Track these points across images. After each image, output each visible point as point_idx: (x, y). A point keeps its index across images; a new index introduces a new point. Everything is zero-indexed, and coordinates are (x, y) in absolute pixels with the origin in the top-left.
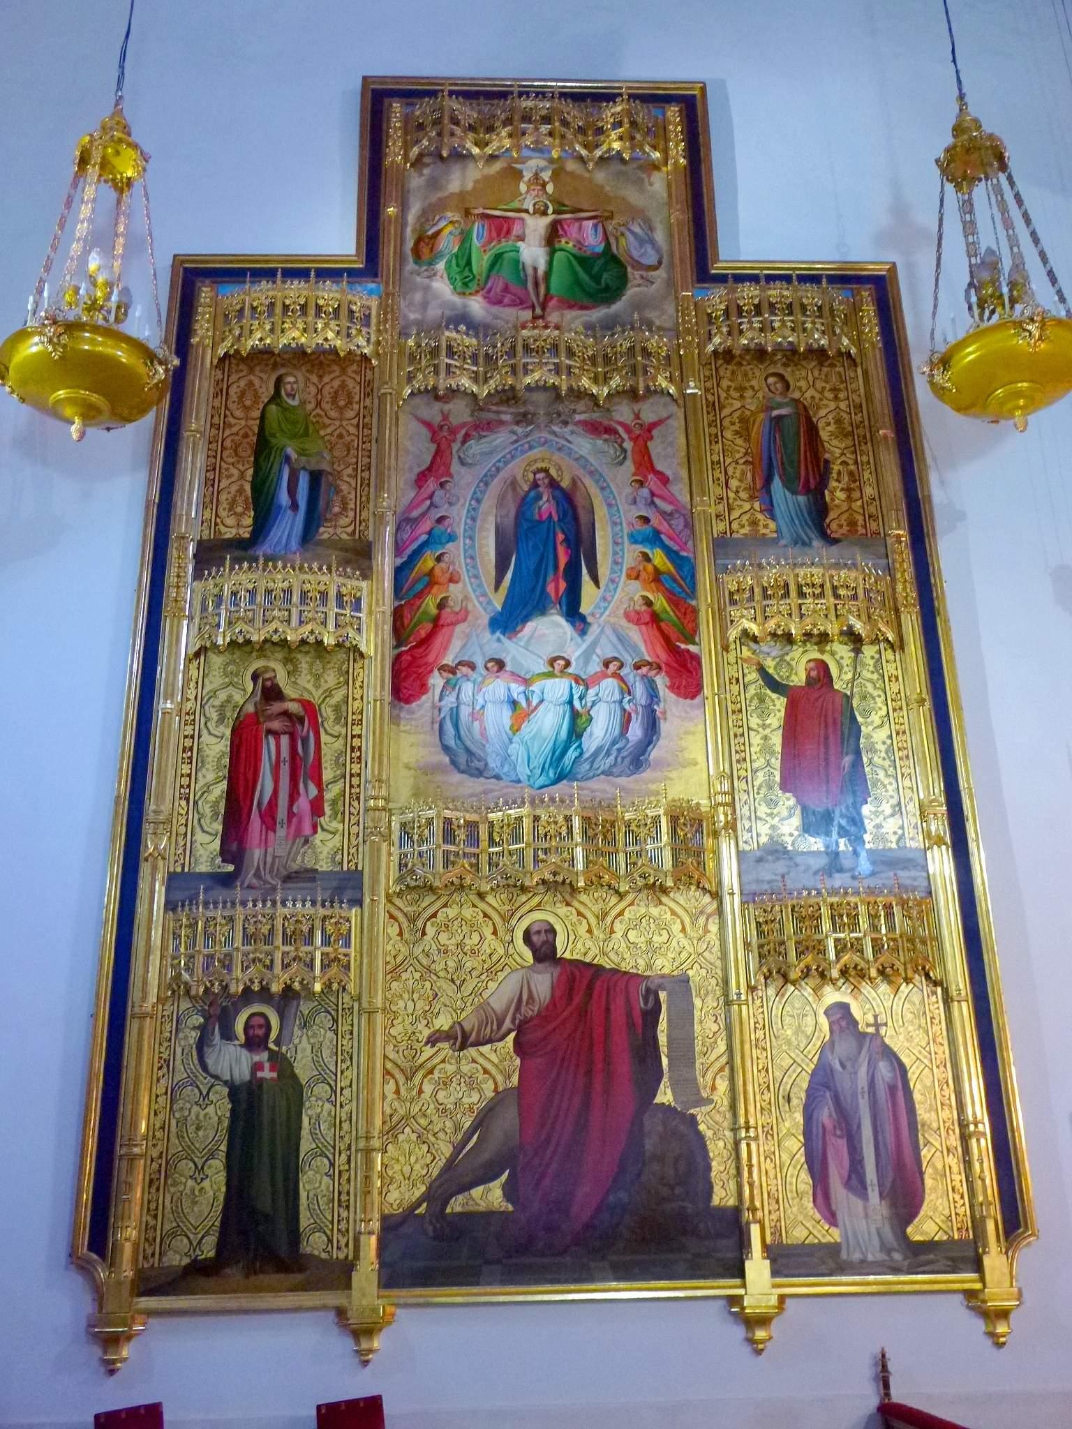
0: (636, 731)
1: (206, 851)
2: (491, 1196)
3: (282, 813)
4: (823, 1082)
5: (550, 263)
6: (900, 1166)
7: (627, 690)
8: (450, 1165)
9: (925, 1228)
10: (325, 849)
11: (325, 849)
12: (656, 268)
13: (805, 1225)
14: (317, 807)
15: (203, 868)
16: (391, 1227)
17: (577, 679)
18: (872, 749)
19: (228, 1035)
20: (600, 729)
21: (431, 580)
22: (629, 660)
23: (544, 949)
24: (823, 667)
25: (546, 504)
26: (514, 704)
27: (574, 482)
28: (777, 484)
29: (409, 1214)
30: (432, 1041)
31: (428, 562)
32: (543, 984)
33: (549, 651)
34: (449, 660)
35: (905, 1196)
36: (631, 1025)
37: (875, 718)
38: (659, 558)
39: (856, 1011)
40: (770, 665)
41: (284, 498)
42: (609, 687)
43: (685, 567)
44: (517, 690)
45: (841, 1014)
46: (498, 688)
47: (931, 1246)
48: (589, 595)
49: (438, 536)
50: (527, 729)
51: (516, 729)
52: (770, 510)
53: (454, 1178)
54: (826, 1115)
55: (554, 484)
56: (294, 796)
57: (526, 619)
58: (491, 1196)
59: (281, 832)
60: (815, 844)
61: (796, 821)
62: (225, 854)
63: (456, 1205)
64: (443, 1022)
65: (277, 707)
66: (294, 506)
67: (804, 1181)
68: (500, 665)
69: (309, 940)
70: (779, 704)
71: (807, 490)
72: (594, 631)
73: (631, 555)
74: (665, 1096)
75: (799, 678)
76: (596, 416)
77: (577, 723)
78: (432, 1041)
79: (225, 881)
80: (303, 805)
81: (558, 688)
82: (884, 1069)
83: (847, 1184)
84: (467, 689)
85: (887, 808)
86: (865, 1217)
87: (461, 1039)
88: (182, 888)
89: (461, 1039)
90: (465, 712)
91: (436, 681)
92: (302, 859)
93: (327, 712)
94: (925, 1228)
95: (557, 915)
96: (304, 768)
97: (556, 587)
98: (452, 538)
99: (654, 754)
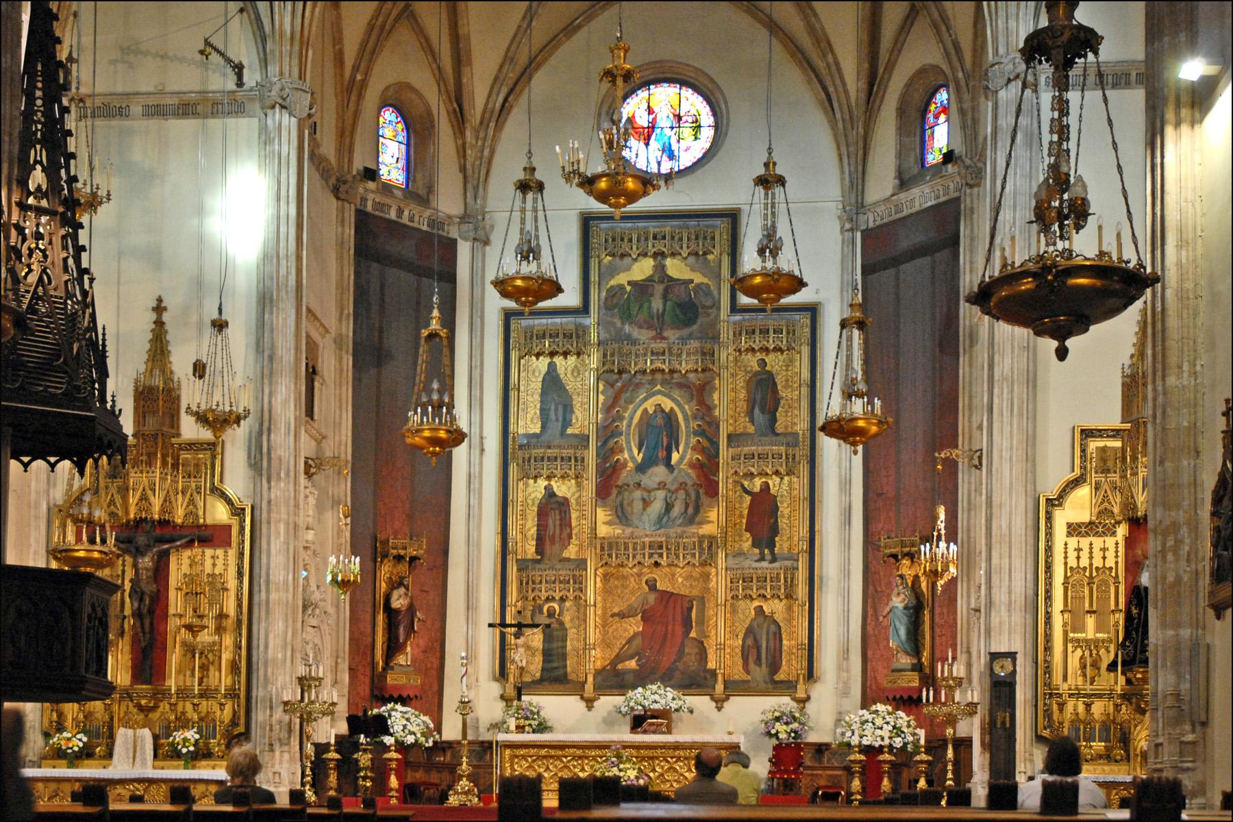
0: (691, 511)
1: (530, 550)
2: (632, 664)
3: (557, 539)
4: (750, 631)
5: (665, 306)
6: (774, 657)
7: (688, 495)
8: (617, 656)
9: (781, 676)
10: (571, 552)
11: (571, 552)
12: (711, 308)
13: (738, 673)
14: (570, 537)
15: (529, 557)
16: (598, 673)
17: (669, 491)
18: (783, 516)
19: (541, 612)
20: (677, 510)
21: (613, 451)
22: (690, 483)
23: (652, 586)
24: (767, 484)
25: (659, 420)
26: (644, 500)
27: (672, 409)
28: (757, 411)
29: (604, 669)
30: (612, 616)
31: (611, 443)
32: (652, 598)
33: (657, 480)
34: (620, 483)
35: (775, 667)
36: (682, 612)
37: (785, 505)
38: (706, 443)
39: (765, 608)
40: (746, 483)
41: (553, 416)
42: (681, 495)
43: (715, 445)
44: (645, 495)
45: (760, 610)
46: (638, 494)
47: (782, 682)
48: (675, 457)
49: (616, 433)
50: (649, 510)
51: (644, 509)
52: (752, 421)
53: (619, 658)
54: (750, 642)
55: (663, 411)
56: (561, 530)
57: (649, 467)
58: (632, 664)
59: (557, 545)
60: (757, 551)
61: (750, 542)
62: (537, 552)
63: (620, 667)
64: (616, 610)
65: (554, 500)
66: (557, 420)
67: (740, 662)
68: (639, 485)
69: (568, 582)
70: (748, 498)
71: (770, 412)
72: (676, 472)
73: (693, 440)
74: (693, 634)
75: (757, 489)
76: (682, 380)
77: (669, 507)
78: (612, 616)
79: (538, 562)
80: (565, 535)
81: (661, 494)
82: (773, 628)
83: (755, 663)
84: (626, 494)
85: (785, 538)
86: (759, 673)
87: (622, 615)
88: (523, 565)
89: (622, 615)
90: (625, 503)
91: (615, 491)
92: (566, 554)
93: (573, 501)
94: (781, 676)
95: (656, 574)
96: (565, 522)
97: (662, 454)
98: (621, 434)
99: (697, 520)
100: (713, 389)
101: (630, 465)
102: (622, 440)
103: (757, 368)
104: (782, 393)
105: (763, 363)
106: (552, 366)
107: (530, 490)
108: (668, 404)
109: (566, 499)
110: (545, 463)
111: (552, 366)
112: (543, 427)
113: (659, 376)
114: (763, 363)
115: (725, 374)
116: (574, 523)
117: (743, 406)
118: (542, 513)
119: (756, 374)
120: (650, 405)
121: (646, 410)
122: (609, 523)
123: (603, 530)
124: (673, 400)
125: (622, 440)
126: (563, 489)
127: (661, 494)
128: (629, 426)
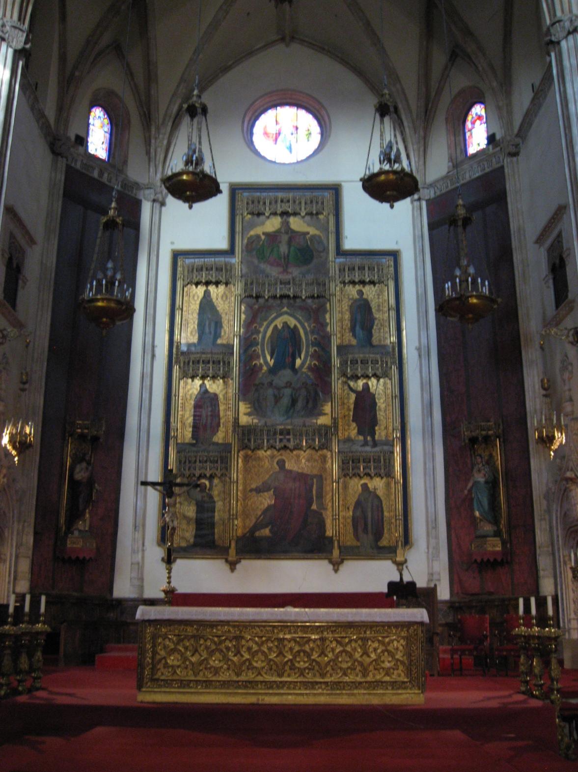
1: (188, 434)
10: (219, 437)
52: (354, 336)
96: (216, 415)
100: (325, 311)
101: (265, 368)
102: (259, 349)
103: (356, 296)
104: (377, 315)
105: (360, 293)
106: (207, 294)
107: (189, 387)
108: (292, 322)
109: (216, 396)
110: (201, 366)
111: (207, 294)
112: (200, 338)
113: (285, 301)
114: (360, 293)
115: (335, 300)
116: (222, 414)
117: (347, 323)
118: (197, 406)
119: (355, 301)
120: (279, 322)
121: (276, 326)
122: (249, 414)
123: (244, 420)
124: (296, 318)
125: (259, 349)
126: (214, 387)
127: (288, 391)
128: (264, 338)
